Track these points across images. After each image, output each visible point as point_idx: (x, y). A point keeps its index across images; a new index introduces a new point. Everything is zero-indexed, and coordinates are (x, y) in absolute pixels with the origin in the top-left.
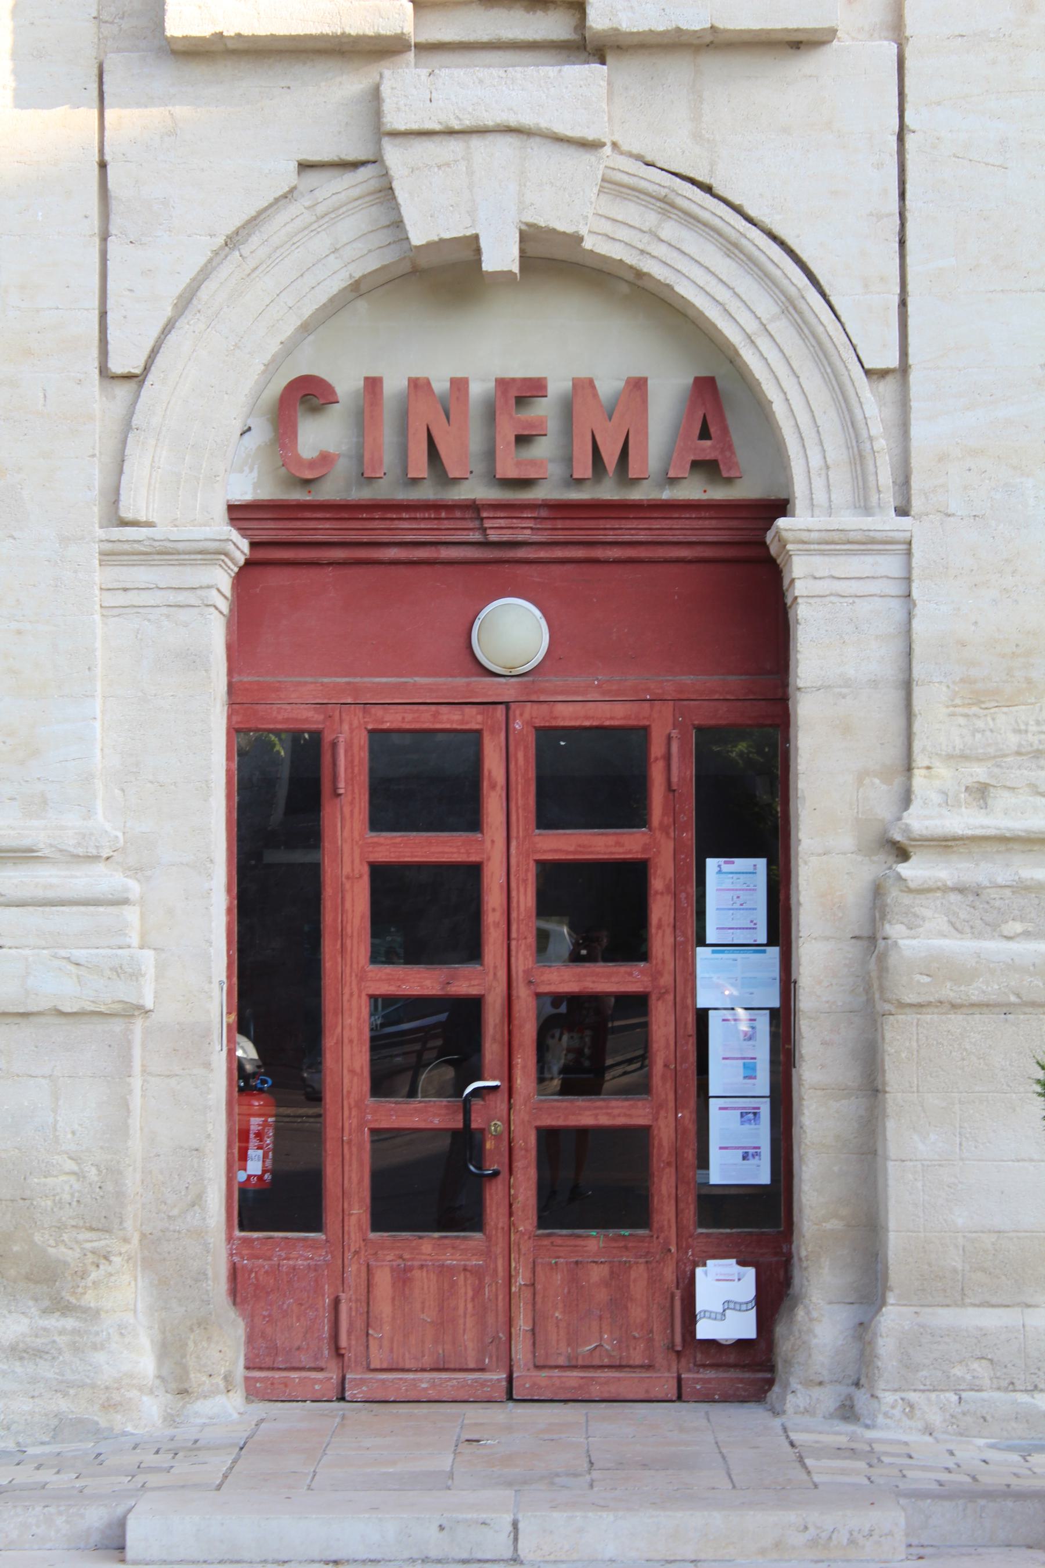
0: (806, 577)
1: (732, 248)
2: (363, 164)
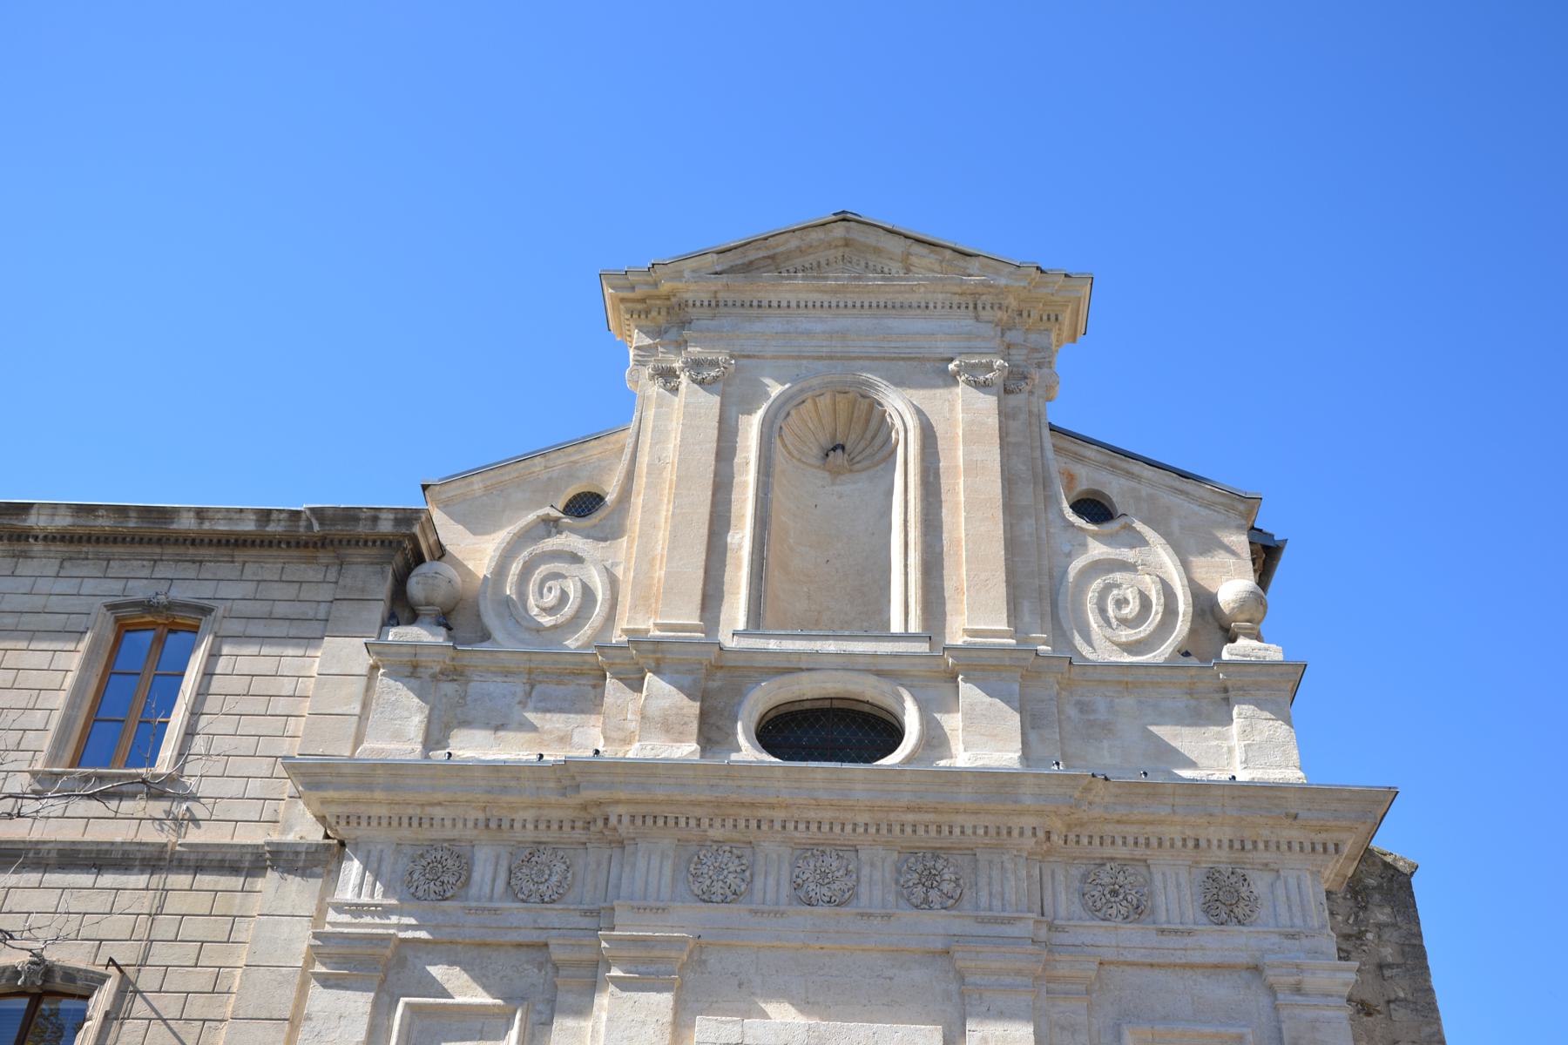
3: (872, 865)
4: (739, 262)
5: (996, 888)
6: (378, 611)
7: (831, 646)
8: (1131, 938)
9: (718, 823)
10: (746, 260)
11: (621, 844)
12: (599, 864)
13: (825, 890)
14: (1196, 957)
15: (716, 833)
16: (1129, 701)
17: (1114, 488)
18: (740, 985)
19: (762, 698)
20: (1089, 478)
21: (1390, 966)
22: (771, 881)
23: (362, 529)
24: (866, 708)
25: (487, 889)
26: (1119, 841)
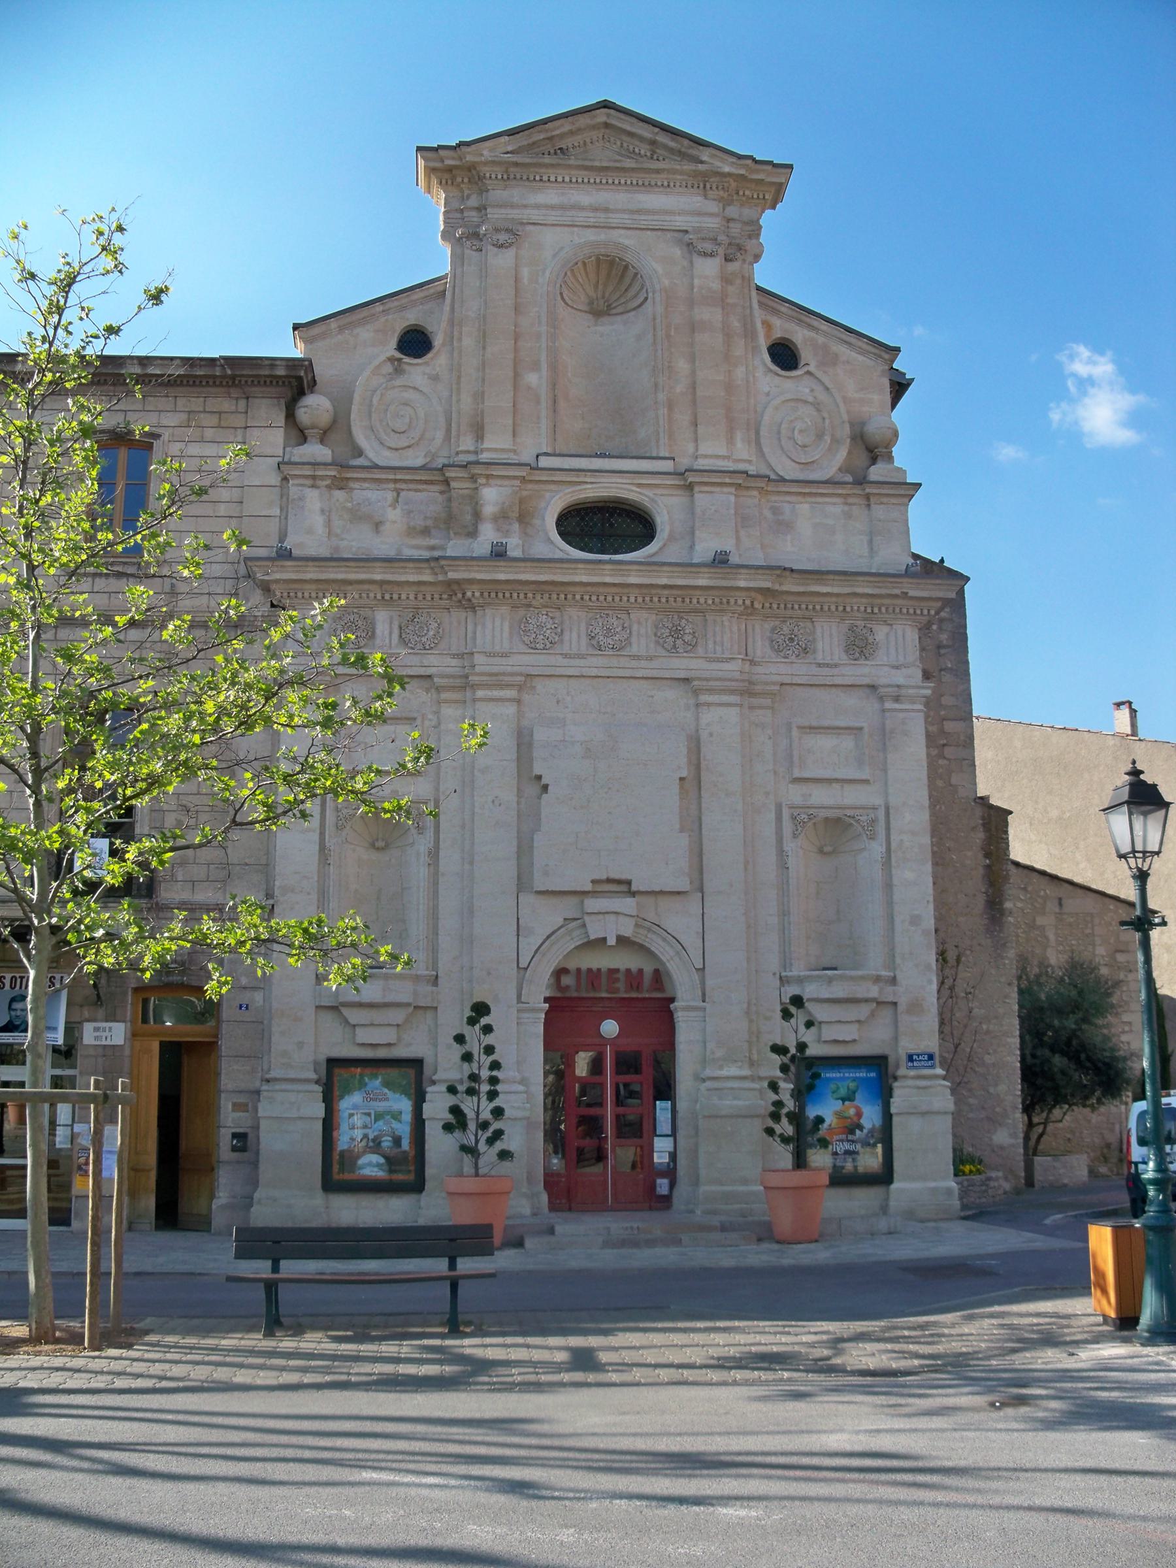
0: (681, 1017)
1: (664, 940)
2: (577, 921)
3: (639, 623)
4: (525, 143)
5: (718, 639)
8: (800, 670)
9: (538, 596)
10: (531, 141)
11: (473, 608)
12: (459, 623)
13: (610, 641)
17: (799, 336)
18: (558, 702)
20: (782, 328)
21: (945, 647)
22: (574, 635)
24: (628, 507)
25: (387, 641)
26: (796, 607)
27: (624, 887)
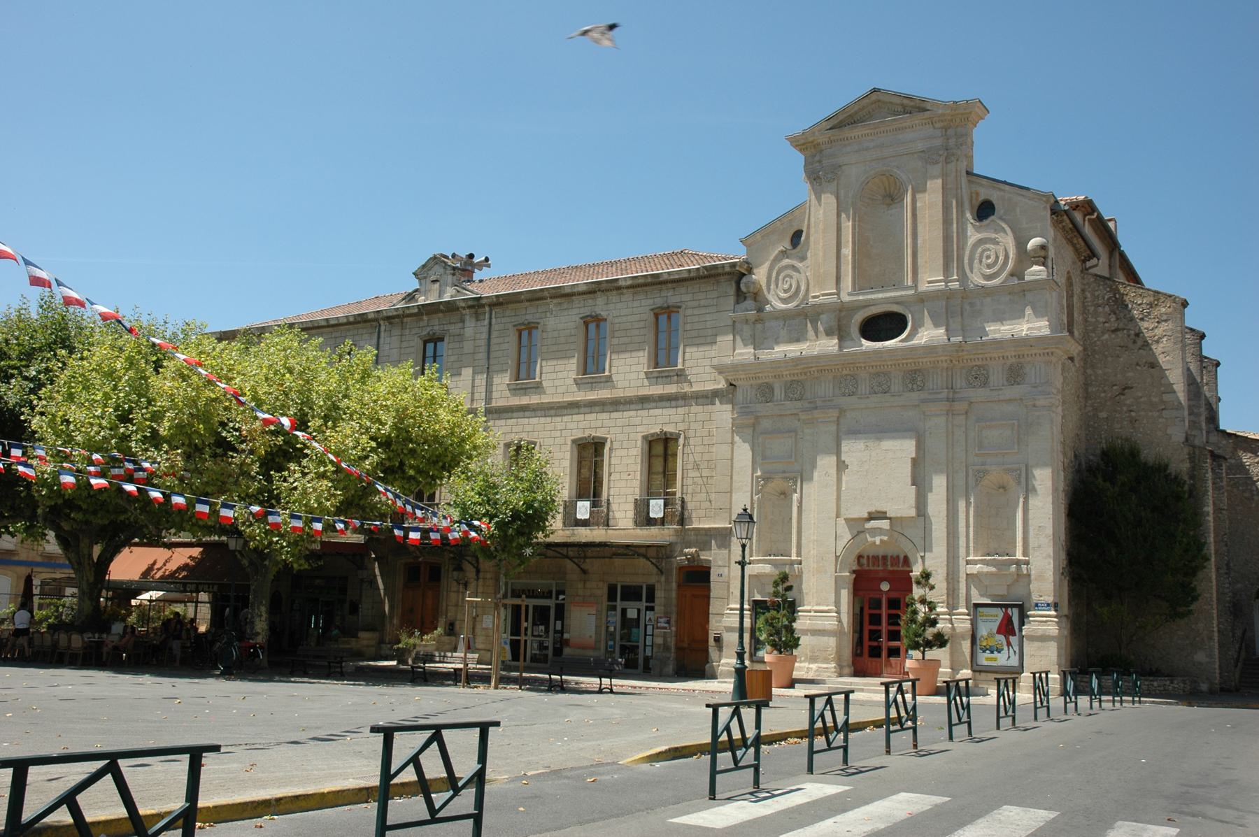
6: (732, 299)
7: (881, 295)
8: (979, 394)
14: (1001, 398)
15: (845, 372)
16: (989, 299)
17: (994, 197)
19: (859, 317)
20: (984, 193)
23: (720, 271)
27: (881, 516)
